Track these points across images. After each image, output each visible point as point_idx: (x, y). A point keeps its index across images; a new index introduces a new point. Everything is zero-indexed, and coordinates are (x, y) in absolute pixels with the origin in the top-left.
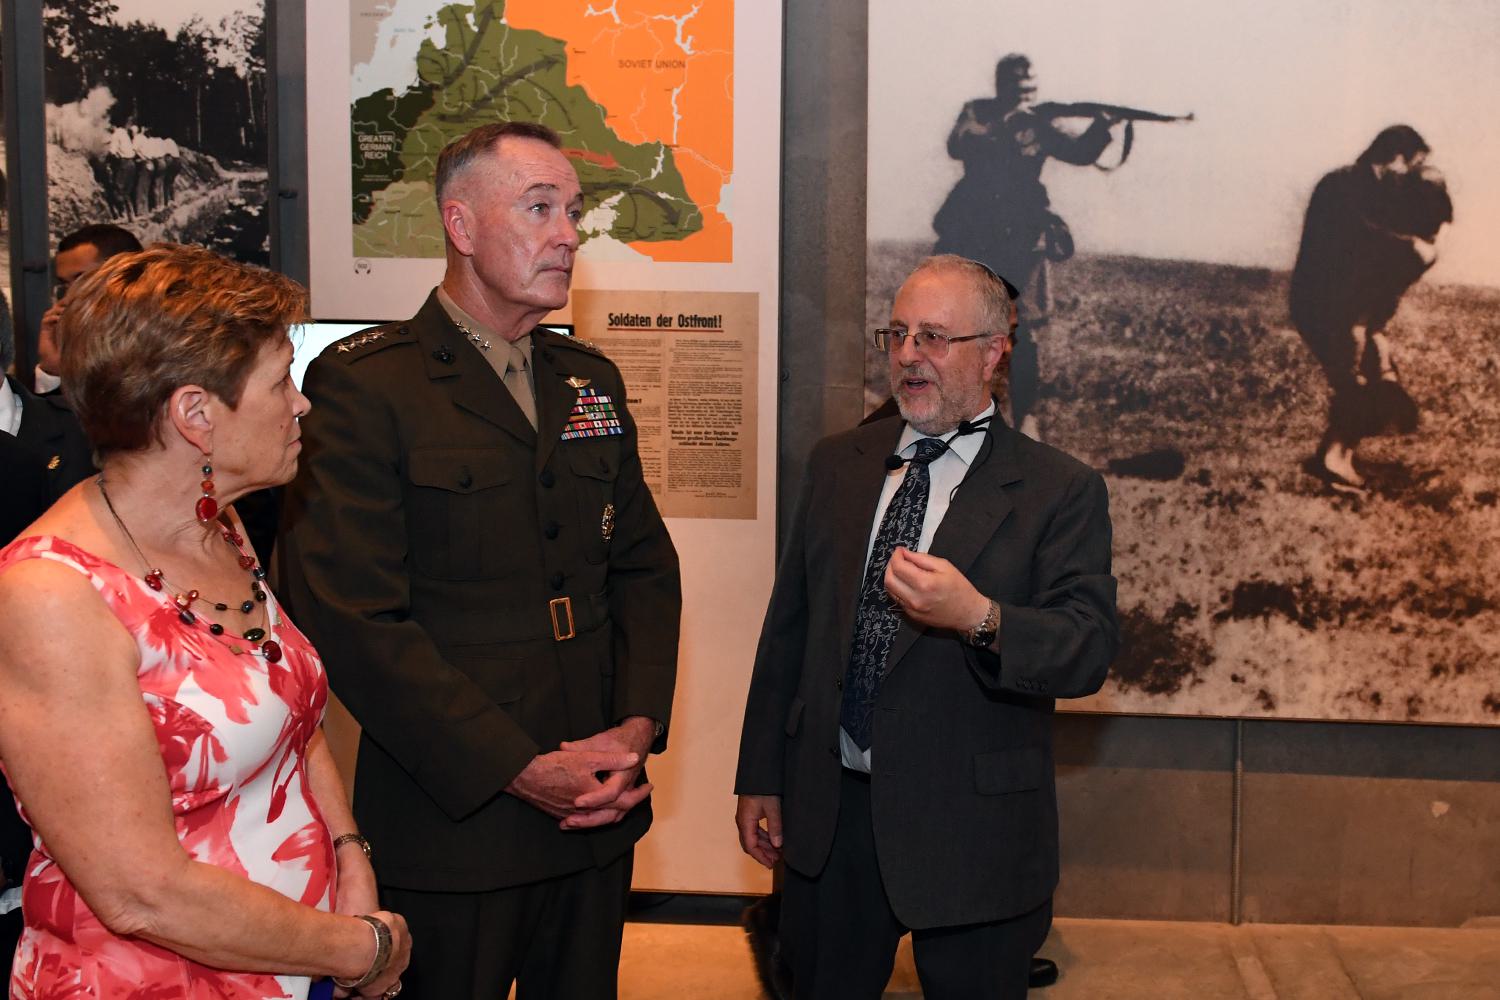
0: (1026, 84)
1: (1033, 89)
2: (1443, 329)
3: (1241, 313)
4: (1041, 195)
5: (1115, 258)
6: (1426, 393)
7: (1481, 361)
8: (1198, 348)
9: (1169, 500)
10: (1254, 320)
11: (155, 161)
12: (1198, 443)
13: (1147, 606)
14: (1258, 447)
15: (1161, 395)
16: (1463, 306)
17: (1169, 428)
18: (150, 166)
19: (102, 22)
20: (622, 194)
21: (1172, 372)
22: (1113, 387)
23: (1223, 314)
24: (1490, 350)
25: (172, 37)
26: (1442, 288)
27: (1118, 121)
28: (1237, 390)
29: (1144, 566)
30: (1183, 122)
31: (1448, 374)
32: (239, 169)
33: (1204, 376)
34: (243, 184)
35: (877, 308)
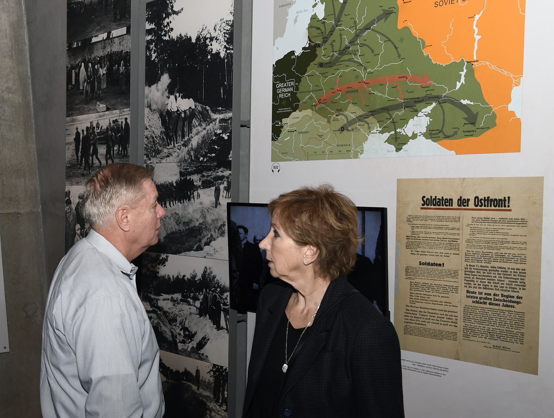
11: (185, 112)
18: (183, 115)
19: (167, 38)
20: (434, 104)
25: (194, 41)
32: (220, 112)
34: (222, 121)
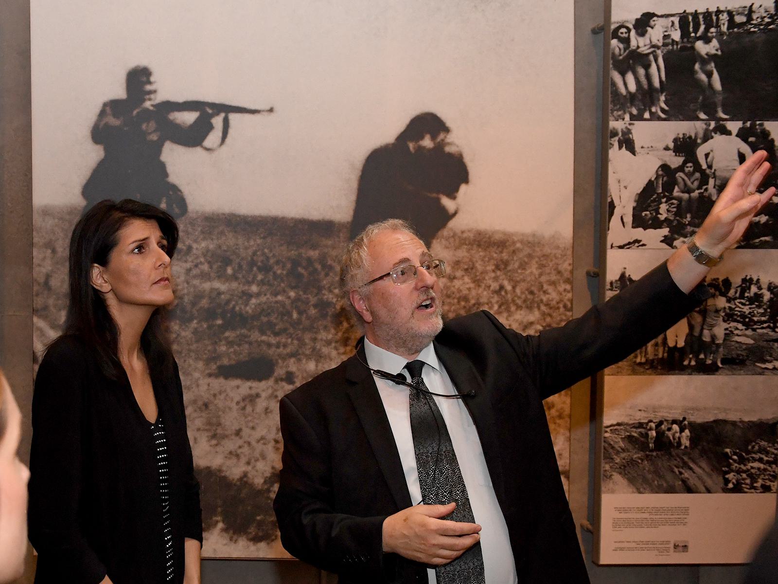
0: (148, 88)
1: (155, 92)
2: (464, 263)
3: (314, 254)
4: (162, 169)
5: (218, 215)
6: (454, 311)
7: (495, 286)
8: (282, 281)
9: (264, 395)
10: (322, 259)
12: (285, 352)
13: (249, 475)
14: (329, 353)
15: (255, 317)
16: (479, 246)
17: (263, 342)
21: (263, 299)
22: (219, 311)
23: (300, 255)
24: (501, 278)
26: (463, 232)
27: (218, 114)
28: (313, 311)
29: (246, 445)
30: (266, 114)
31: (471, 297)
33: (288, 302)
35: (41, 256)
